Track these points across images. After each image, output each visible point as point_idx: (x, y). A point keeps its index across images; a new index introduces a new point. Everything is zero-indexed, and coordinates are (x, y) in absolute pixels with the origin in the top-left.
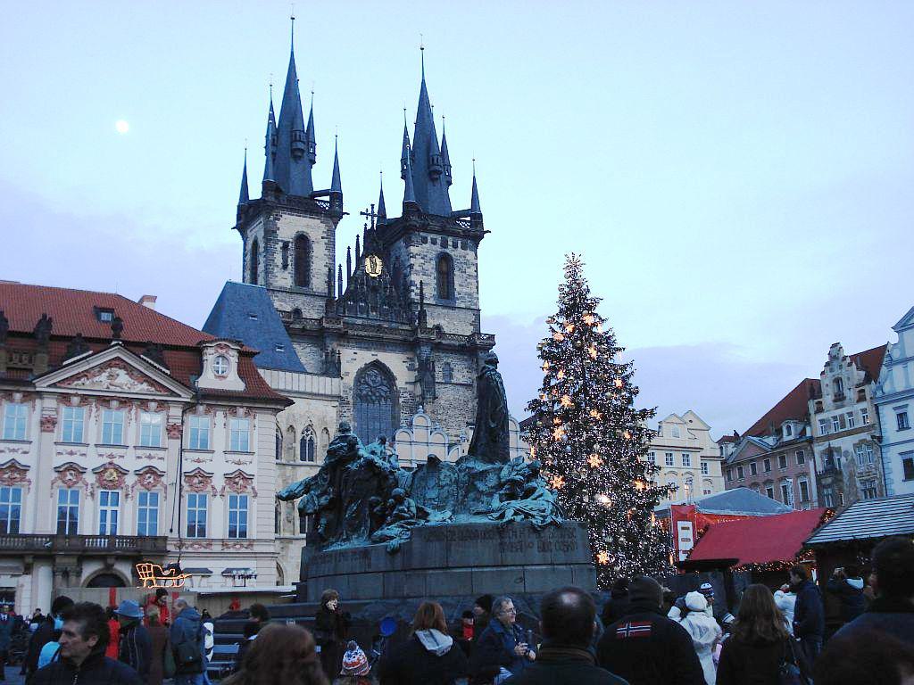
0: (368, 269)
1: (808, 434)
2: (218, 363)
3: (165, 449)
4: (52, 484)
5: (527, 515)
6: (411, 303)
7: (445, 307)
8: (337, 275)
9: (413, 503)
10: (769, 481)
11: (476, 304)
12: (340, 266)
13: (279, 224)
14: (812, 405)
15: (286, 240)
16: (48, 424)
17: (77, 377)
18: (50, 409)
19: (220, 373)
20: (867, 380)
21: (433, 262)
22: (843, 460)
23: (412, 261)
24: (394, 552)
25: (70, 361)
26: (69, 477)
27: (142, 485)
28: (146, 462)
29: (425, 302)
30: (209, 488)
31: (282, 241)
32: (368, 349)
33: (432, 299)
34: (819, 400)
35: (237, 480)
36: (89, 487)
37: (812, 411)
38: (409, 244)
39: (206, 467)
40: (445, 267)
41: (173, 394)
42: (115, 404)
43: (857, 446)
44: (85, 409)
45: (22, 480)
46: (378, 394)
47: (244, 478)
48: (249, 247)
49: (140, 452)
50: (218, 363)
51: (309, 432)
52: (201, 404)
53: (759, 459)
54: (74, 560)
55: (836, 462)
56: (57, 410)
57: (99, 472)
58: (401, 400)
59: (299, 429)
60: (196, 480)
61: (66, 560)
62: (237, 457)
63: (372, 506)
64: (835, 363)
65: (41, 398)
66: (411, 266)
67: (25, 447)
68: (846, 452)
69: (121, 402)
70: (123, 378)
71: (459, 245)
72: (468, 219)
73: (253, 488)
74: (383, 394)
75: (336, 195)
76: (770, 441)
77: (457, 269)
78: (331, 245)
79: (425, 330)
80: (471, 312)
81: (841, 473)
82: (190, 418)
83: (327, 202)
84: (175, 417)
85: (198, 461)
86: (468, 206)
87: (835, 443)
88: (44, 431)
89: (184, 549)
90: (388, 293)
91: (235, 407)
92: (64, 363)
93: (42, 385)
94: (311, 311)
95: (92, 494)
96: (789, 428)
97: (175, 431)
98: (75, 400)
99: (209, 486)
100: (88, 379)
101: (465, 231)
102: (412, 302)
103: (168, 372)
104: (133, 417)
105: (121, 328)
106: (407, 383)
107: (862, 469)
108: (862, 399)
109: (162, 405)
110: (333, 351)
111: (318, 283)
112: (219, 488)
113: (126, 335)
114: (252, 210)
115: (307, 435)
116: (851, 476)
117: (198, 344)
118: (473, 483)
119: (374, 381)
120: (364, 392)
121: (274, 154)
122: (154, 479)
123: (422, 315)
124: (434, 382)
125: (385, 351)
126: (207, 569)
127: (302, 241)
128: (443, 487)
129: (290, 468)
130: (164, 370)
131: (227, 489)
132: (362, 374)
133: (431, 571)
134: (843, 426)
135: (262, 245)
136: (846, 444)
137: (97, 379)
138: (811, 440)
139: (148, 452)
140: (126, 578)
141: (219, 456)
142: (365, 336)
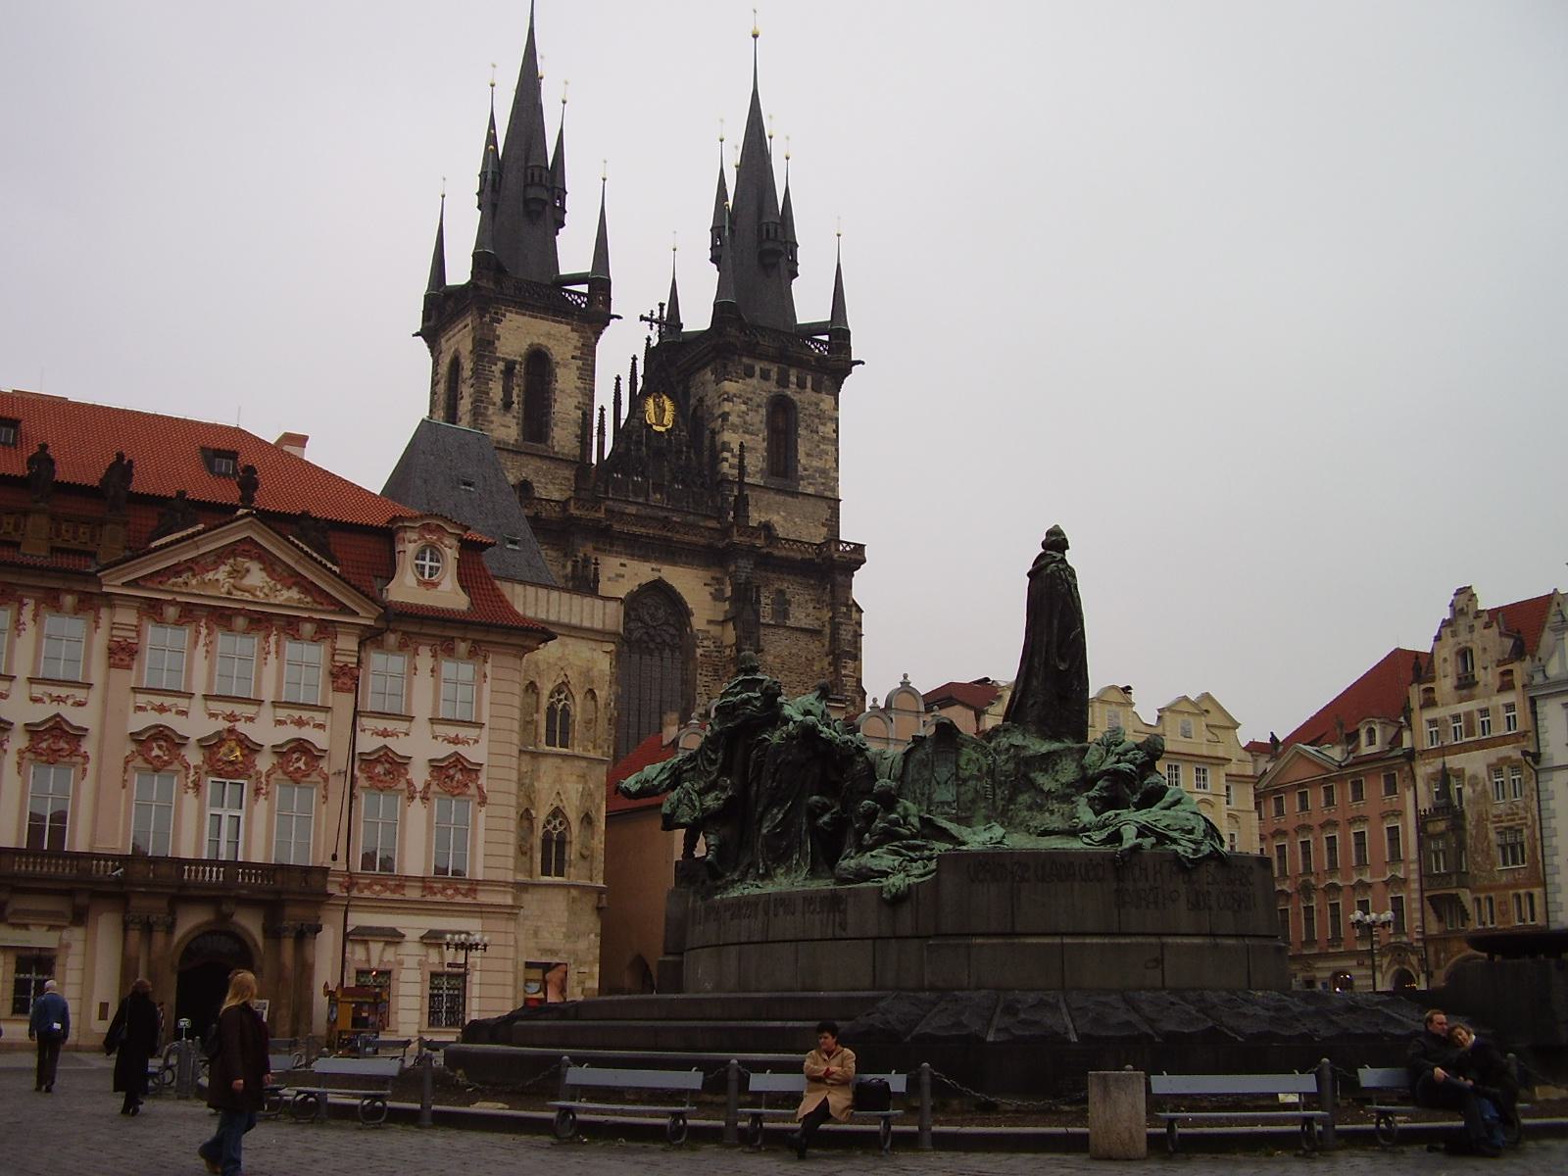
0: (651, 416)
1: (1407, 743)
2: (424, 559)
3: (326, 709)
4: (127, 763)
5: (1162, 839)
6: (722, 480)
7: (779, 491)
8: (596, 424)
9: (913, 808)
10: (1331, 824)
11: (835, 489)
12: (602, 409)
13: (500, 329)
14: (1415, 694)
15: (511, 357)
16: (122, 654)
17: (176, 570)
18: (123, 627)
19: (427, 577)
20: (1520, 652)
21: (763, 411)
22: (1467, 791)
23: (727, 407)
24: (898, 900)
25: (163, 541)
26: (156, 752)
27: (285, 773)
28: (291, 732)
29: (746, 480)
30: (402, 785)
31: (503, 359)
32: (645, 558)
33: (759, 476)
34: (1428, 685)
35: (452, 772)
36: (192, 772)
37: (1415, 703)
38: (721, 376)
40: (783, 425)
42: (240, 622)
43: (1495, 769)
44: (187, 632)
45: (74, 752)
46: (658, 640)
47: (464, 770)
48: (444, 369)
49: (282, 714)
50: (424, 559)
51: (562, 696)
52: (394, 631)
53: (1313, 784)
54: (163, 903)
55: (1454, 794)
56: (138, 630)
57: (210, 746)
58: (699, 651)
59: (546, 688)
60: (379, 769)
62: (452, 731)
63: (814, 813)
64: (1462, 623)
65: (112, 606)
66: (725, 416)
67: (80, 694)
68: (1474, 777)
69: (251, 621)
70: (256, 577)
71: (809, 385)
72: (826, 338)
73: (479, 788)
74: (668, 638)
75: (599, 282)
76: (1336, 753)
77: (803, 424)
78: (588, 372)
79: (746, 529)
80: (824, 504)
81: (1461, 815)
82: (377, 660)
83: (583, 294)
84: (346, 652)
85: (385, 734)
86: (825, 316)
87: (1454, 762)
88: (112, 666)
89: (355, 893)
90: (682, 463)
91: (453, 638)
92: (153, 545)
93: (112, 584)
94: (550, 487)
96: (1371, 732)
97: (345, 678)
98: (171, 612)
99: (403, 781)
100: (194, 576)
101: (820, 358)
102: (725, 480)
103: (335, 568)
104: (273, 648)
105: (255, 486)
106: (710, 622)
107: (1501, 807)
108: (1506, 686)
109: (325, 631)
110: (586, 560)
111: (563, 437)
112: (419, 786)
113: (264, 500)
114: (451, 303)
115: (560, 701)
116: (1481, 820)
117: (387, 523)
118: (1025, 776)
119: (652, 616)
120: (636, 635)
121: (495, 206)
122: (305, 764)
123: (742, 504)
124: (758, 623)
125: (674, 563)
126: (394, 929)
127: (539, 362)
128: (965, 781)
130: (329, 565)
131: (434, 787)
132: (632, 604)
133: (979, 941)
134: (1470, 732)
135: (467, 366)
136: (1474, 763)
137: (210, 576)
138: (1411, 755)
139: (296, 714)
140: (254, 940)
141: (421, 728)
142: (641, 536)
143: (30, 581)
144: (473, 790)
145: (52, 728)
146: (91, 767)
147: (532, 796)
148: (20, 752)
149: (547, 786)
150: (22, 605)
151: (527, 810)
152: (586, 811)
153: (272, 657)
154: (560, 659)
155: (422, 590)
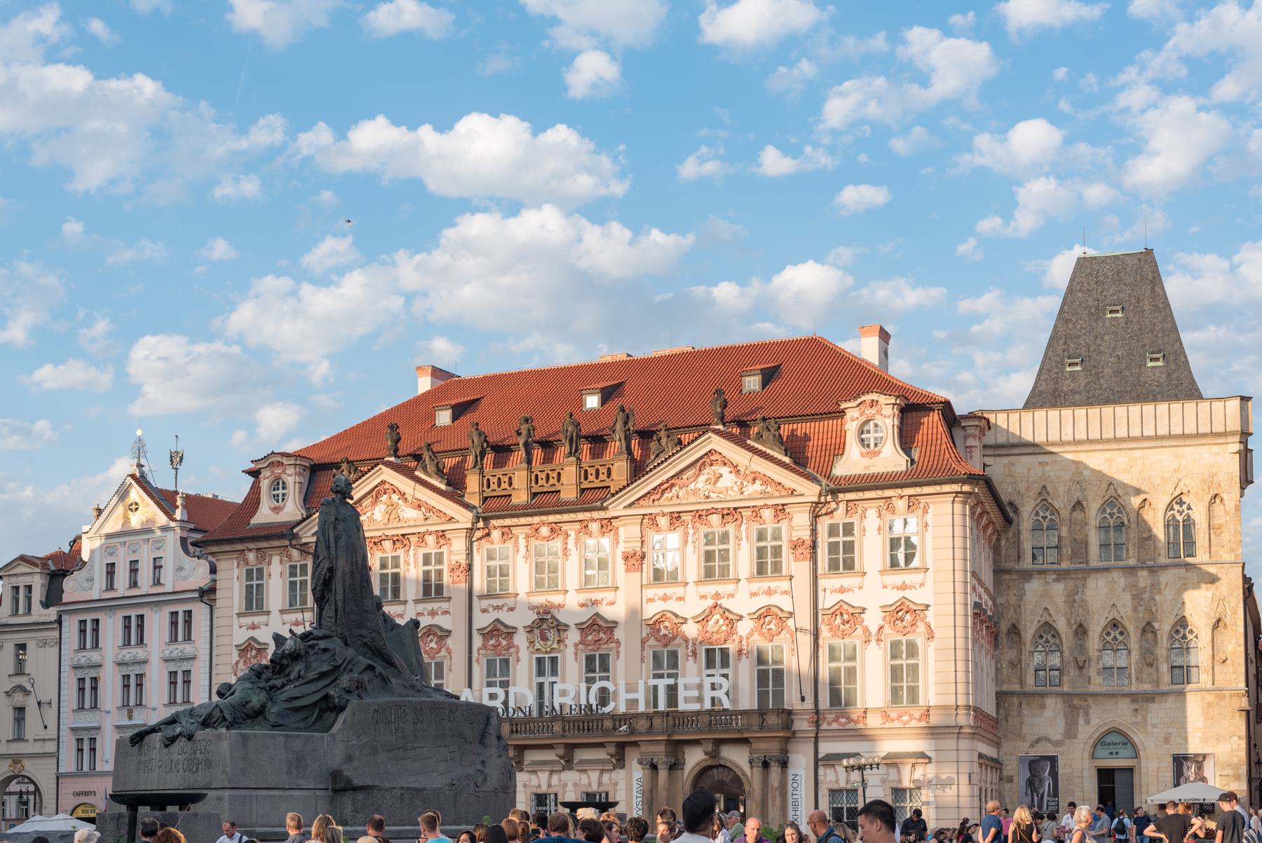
4: (643, 642)
27: (762, 634)
28: (763, 601)
30: (859, 631)
39: (854, 599)
41: (792, 492)
51: (1184, 507)
61: (652, 748)
70: (728, 479)
85: (842, 590)
89: (824, 726)
93: (616, 508)
95: (694, 653)
100: (681, 488)
104: (744, 536)
112: (874, 630)
129: (1143, 574)
131: (887, 630)
137: (692, 486)
143: (566, 517)
144: (921, 627)
145: (592, 625)
146: (622, 649)
147: (1154, 609)
148: (576, 645)
149: (1169, 597)
150: (568, 536)
151: (1149, 623)
152: (1217, 616)
153: (744, 541)
154: (1175, 471)
155: (866, 461)
